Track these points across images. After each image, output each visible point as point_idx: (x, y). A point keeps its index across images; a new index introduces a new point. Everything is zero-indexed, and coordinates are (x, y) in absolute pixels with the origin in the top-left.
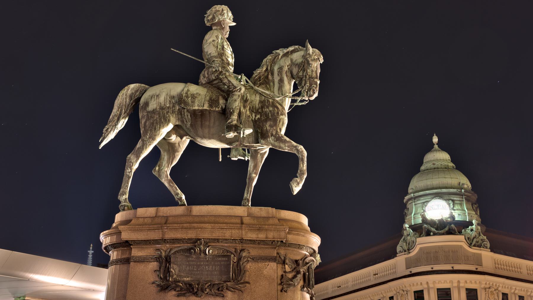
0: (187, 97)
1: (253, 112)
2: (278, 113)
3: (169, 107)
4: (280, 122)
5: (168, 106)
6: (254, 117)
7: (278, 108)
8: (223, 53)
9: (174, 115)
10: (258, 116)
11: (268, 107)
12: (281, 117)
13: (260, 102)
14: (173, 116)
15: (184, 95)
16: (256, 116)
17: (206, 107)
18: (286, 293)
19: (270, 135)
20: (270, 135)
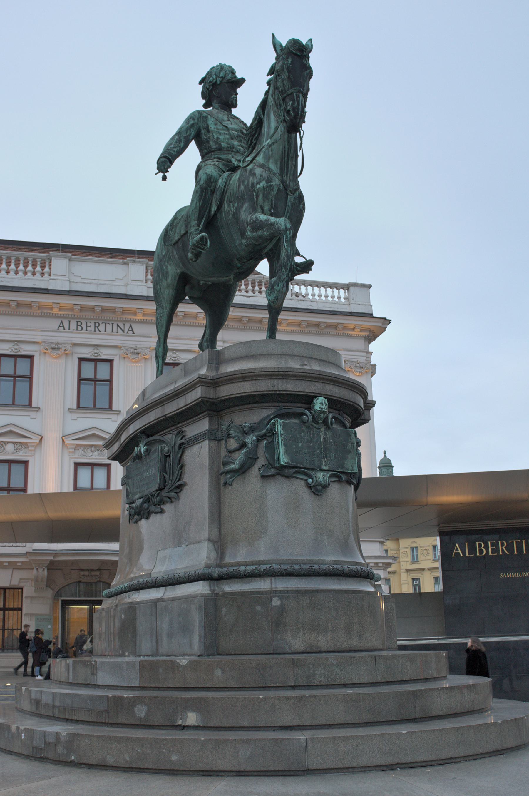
0: (171, 230)
1: (231, 202)
2: (253, 184)
3: (165, 256)
4: (257, 196)
5: (164, 254)
6: (232, 208)
7: (254, 174)
8: (209, 138)
9: (171, 263)
10: (236, 205)
11: (243, 182)
12: (258, 186)
13: (239, 178)
14: (170, 265)
15: (169, 229)
16: (233, 206)
17: (183, 232)
18: (230, 488)
19: (246, 225)
20: (246, 225)
